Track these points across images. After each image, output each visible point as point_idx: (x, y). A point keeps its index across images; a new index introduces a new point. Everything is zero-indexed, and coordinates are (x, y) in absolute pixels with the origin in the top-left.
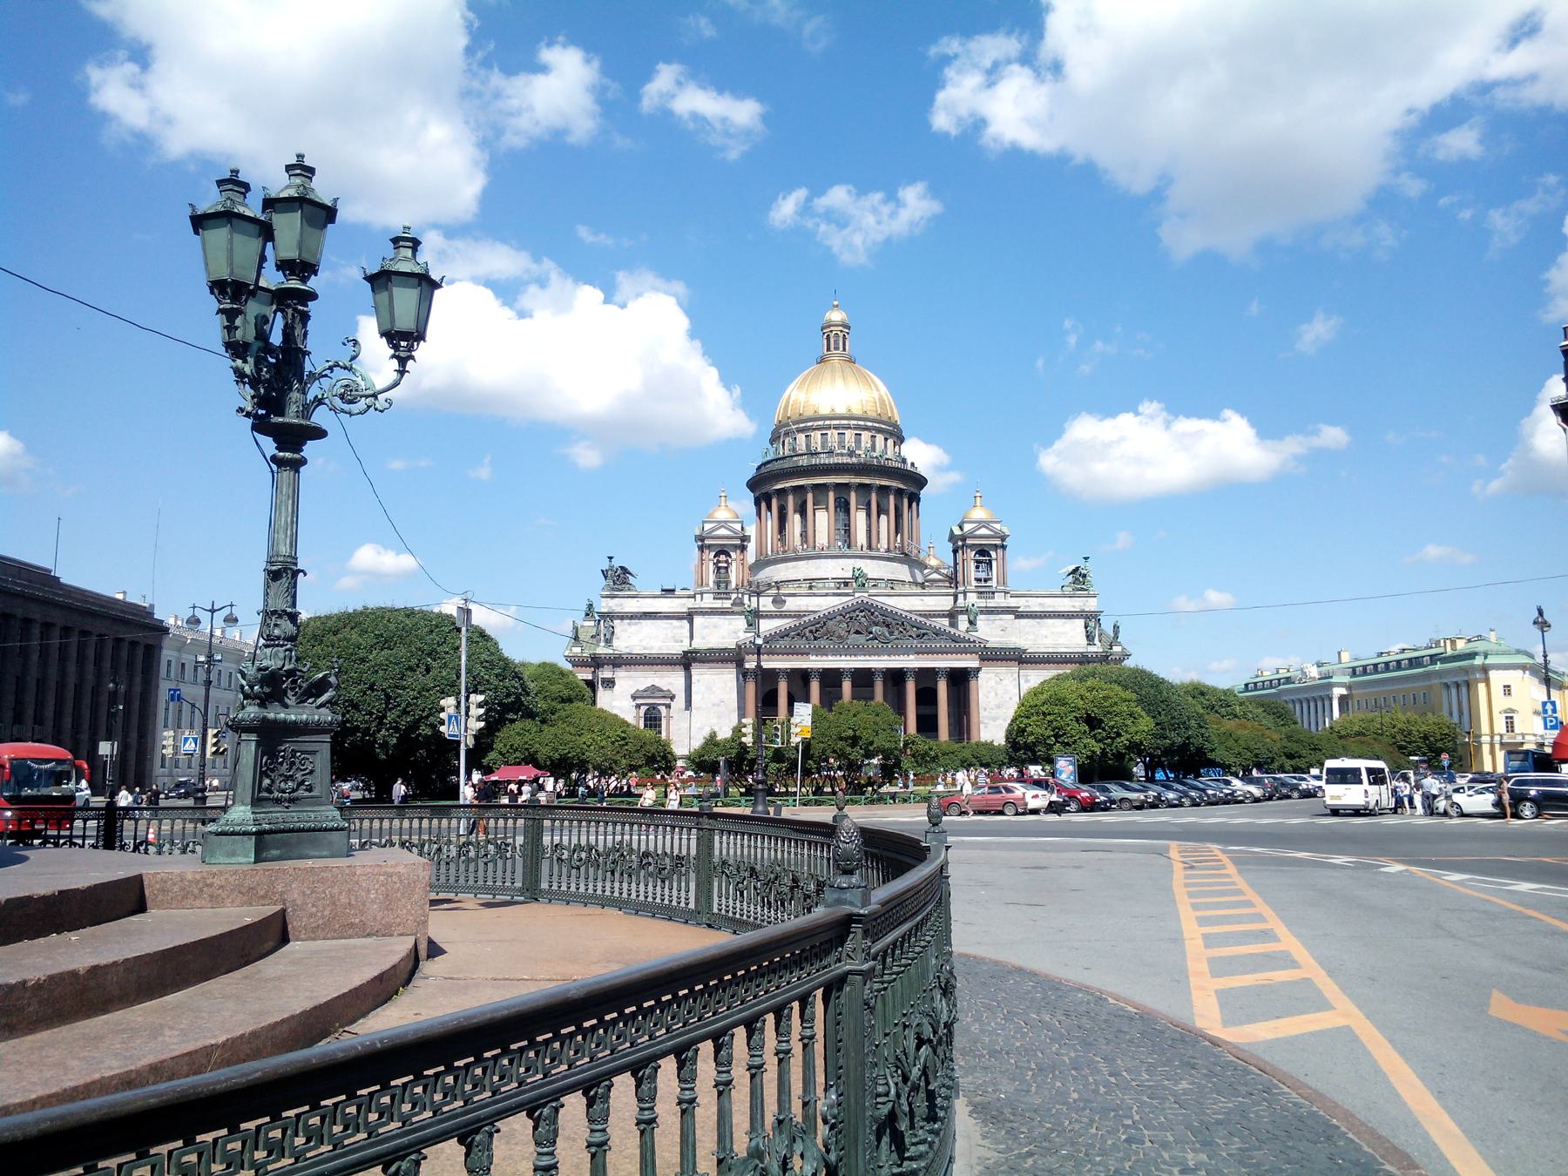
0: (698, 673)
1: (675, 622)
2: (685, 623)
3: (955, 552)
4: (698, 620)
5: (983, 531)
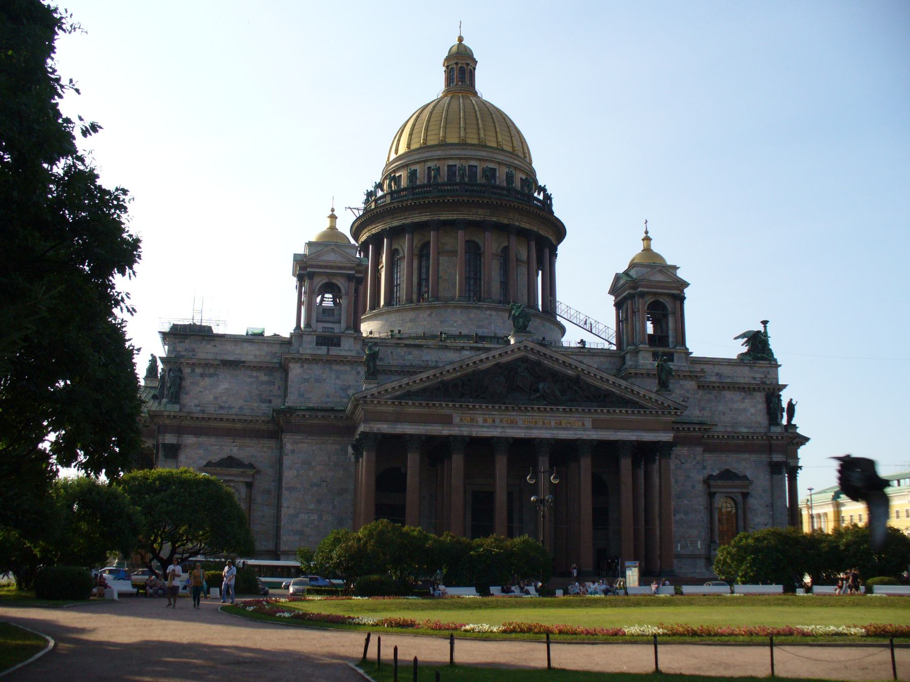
0: (289, 442)
1: (263, 377)
2: (278, 375)
3: (618, 305)
4: (295, 370)
5: (660, 278)
